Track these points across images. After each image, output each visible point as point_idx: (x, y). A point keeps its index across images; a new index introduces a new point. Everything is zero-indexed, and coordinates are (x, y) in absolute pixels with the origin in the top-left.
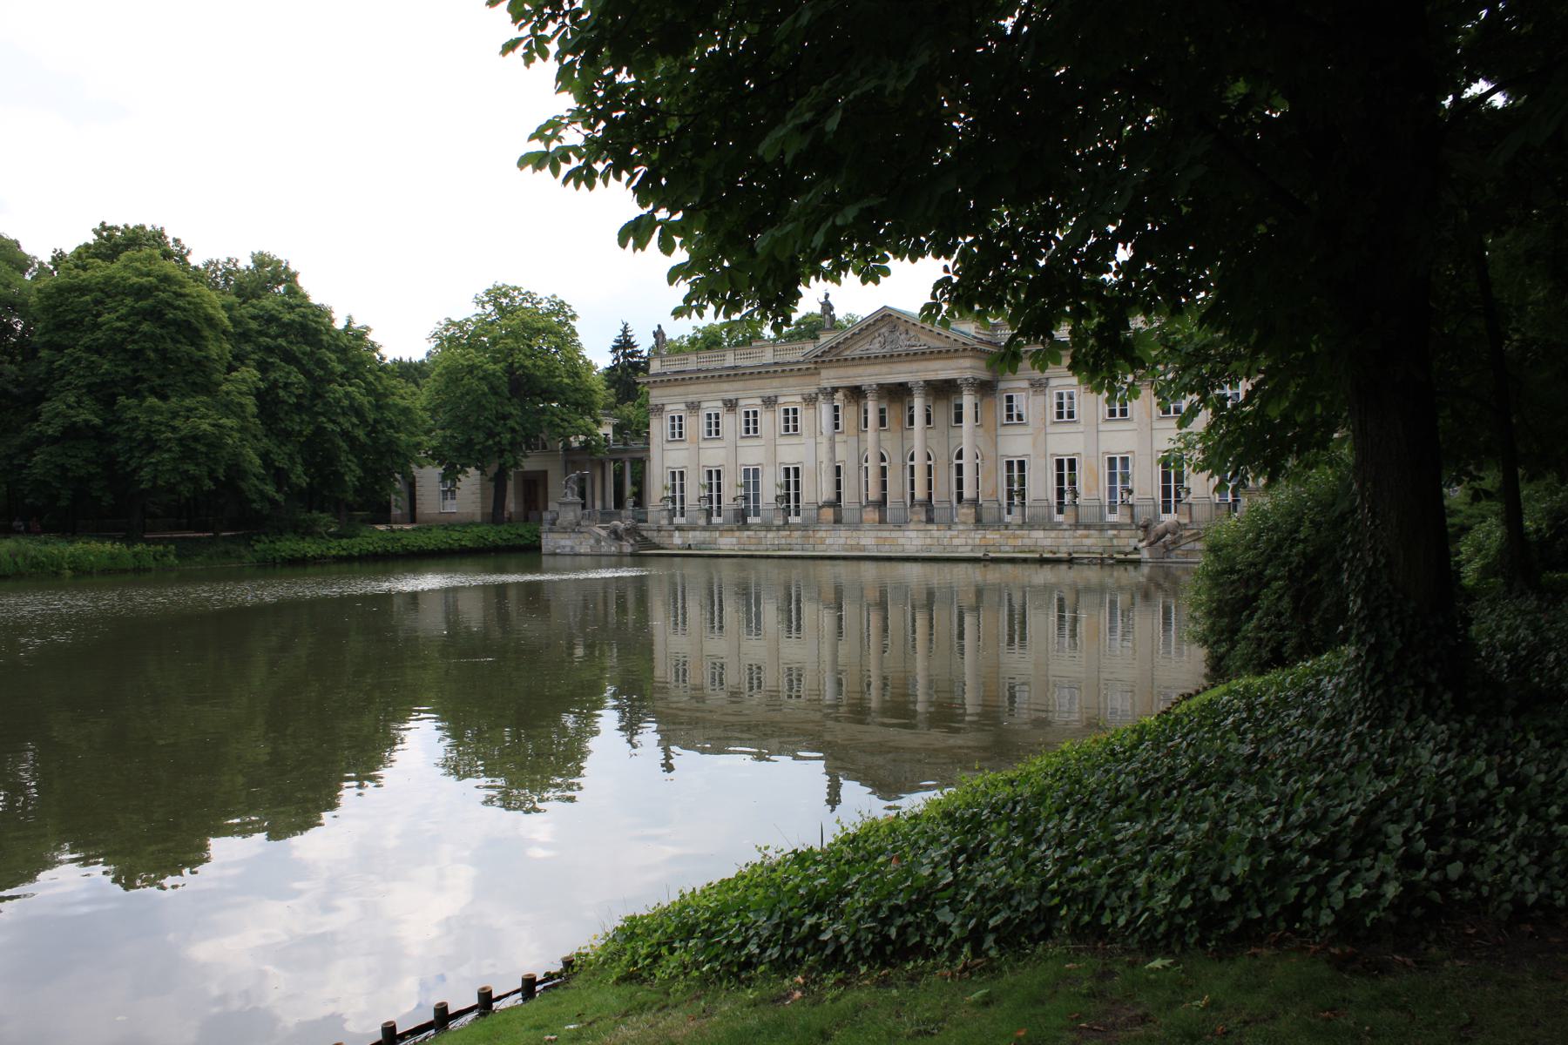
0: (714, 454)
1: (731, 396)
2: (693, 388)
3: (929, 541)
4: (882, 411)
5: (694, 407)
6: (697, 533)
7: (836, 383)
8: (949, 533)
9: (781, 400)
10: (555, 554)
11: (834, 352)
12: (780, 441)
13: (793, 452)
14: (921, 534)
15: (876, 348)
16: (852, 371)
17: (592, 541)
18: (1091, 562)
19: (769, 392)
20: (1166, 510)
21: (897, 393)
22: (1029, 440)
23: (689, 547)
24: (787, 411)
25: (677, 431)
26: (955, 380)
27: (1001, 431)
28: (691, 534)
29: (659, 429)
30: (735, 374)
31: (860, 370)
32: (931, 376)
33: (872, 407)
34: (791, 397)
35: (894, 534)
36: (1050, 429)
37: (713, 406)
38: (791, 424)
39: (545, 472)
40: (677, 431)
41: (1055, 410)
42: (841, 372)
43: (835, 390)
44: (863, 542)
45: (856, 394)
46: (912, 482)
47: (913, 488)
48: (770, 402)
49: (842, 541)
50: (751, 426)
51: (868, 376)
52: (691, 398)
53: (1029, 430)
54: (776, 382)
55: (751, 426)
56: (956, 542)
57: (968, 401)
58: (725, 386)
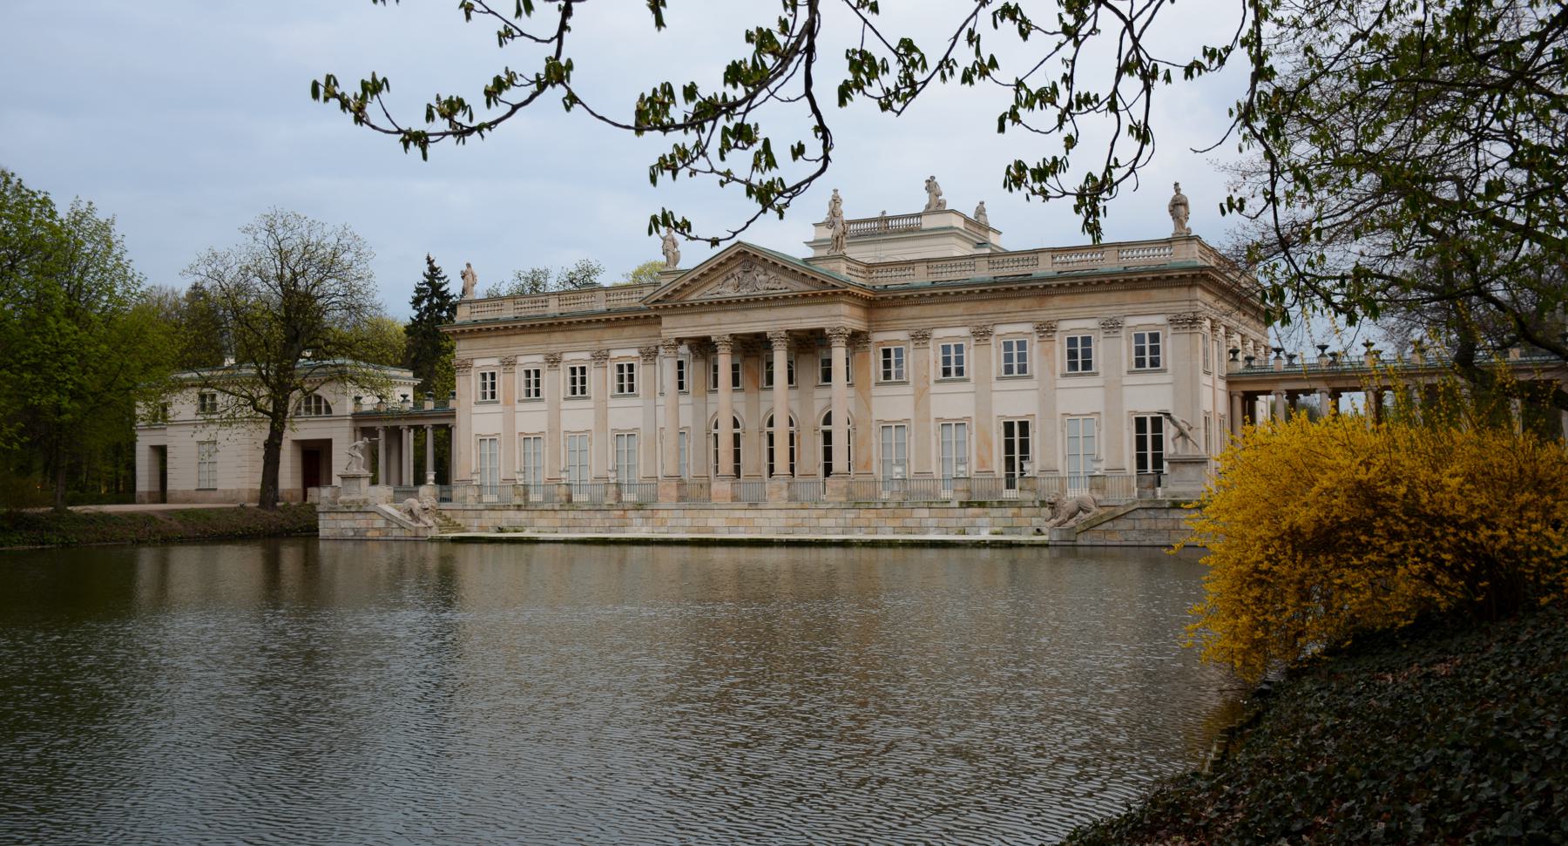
1: (553, 349)
3: (791, 522)
4: (735, 367)
6: (511, 514)
8: (814, 513)
9: (614, 354)
11: (677, 297)
12: (612, 403)
14: (782, 514)
15: (729, 292)
16: (697, 319)
21: (753, 348)
22: (911, 399)
23: (501, 530)
24: (621, 368)
25: (489, 389)
26: (822, 330)
27: (876, 391)
29: (467, 387)
31: (709, 318)
33: (724, 361)
34: (625, 348)
35: (750, 514)
36: (934, 388)
37: (531, 359)
38: (626, 380)
39: (329, 442)
40: (489, 389)
41: (941, 366)
43: (680, 341)
44: (712, 523)
45: (703, 347)
46: (771, 452)
47: (771, 458)
48: (601, 357)
49: (687, 522)
50: (578, 383)
51: (720, 326)
53: (908, 390)
55: (578, 383)
56: (823, 522)
57: (839, 354)
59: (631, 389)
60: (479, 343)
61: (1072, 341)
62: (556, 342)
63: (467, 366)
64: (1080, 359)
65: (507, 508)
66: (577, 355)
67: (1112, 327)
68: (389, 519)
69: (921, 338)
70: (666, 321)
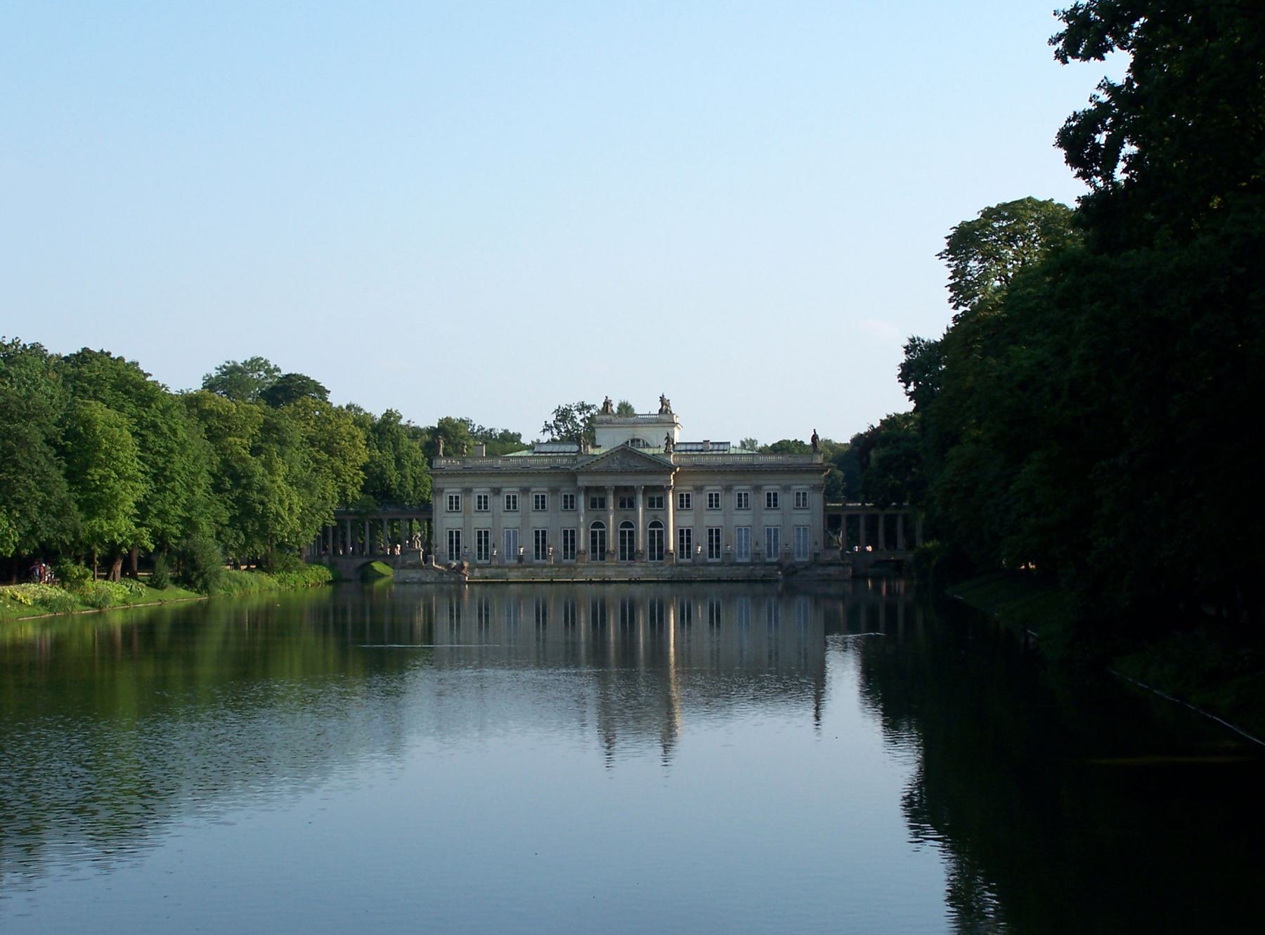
0: (483, 521)
2: (467, 479)
5: (468, 491)
7: (587, 484)
10: (405, 583)
12: (532, 514)
13: (539, 521)
15: (615, 466)
16: (598, 478)
17: (436, 574)
18: (743, 581)
19: (526, 485)
20: (566, 558)
28: (487, 571)
29: (441, 504)
30: (499, 473)
32: (648, 484)
38: (540, 504)
40: (454, 504)
42: (590, 478)
48: (525, 491)
50: (511, 504)
51: (609, 481)
52: (466, 485)
54: (530, 479)
58: (492, 479)
59: (543, 507)
60: (448, 480)
61: (769, 495)
62: (497, 482)
63: (441, 491)
64: (773, 501)
65: (489, 566)
66: (511, 489)
67: (786, 489)
68: (441, 573)
69: (699, 489)
70: (580, 478)
